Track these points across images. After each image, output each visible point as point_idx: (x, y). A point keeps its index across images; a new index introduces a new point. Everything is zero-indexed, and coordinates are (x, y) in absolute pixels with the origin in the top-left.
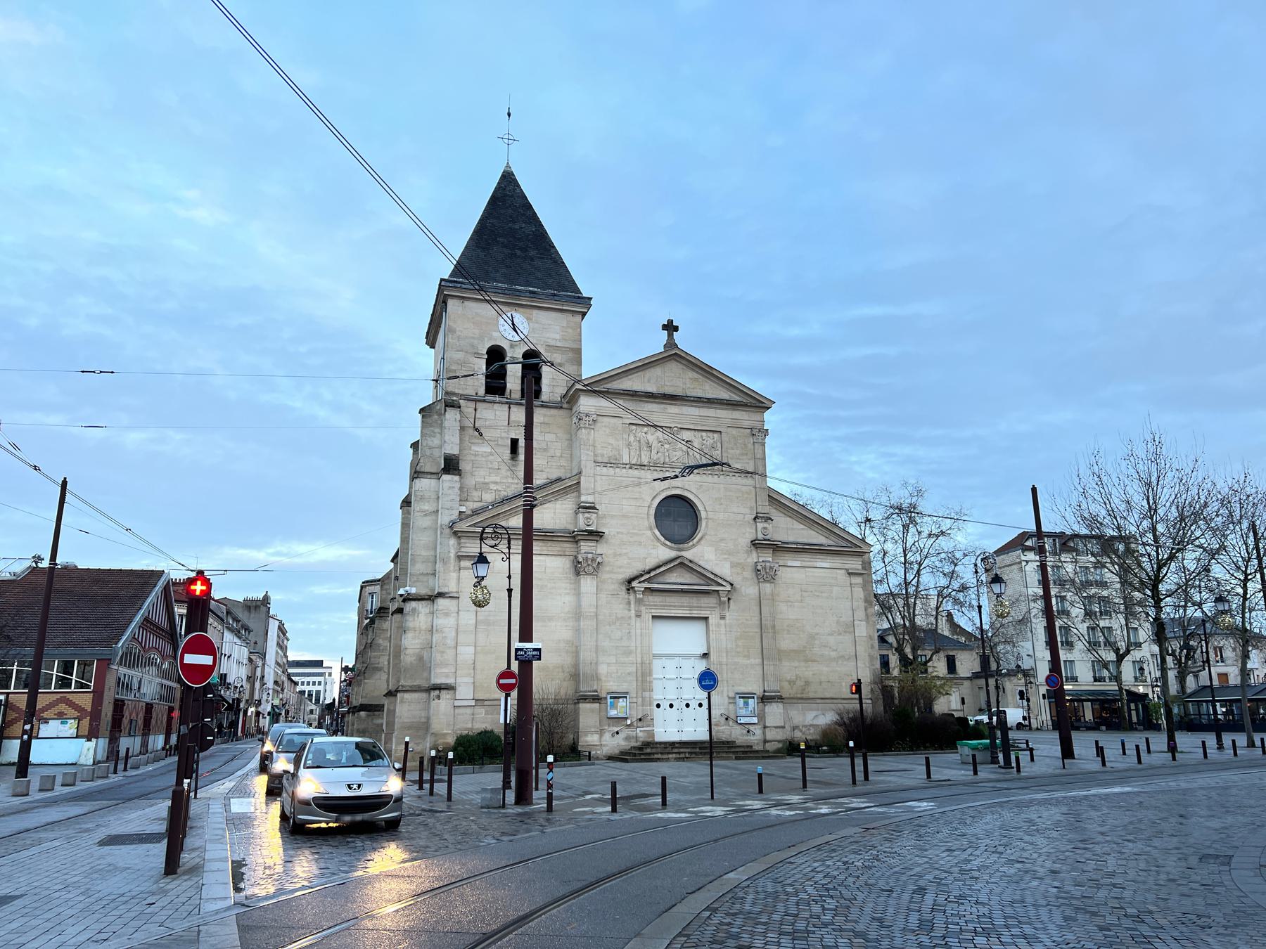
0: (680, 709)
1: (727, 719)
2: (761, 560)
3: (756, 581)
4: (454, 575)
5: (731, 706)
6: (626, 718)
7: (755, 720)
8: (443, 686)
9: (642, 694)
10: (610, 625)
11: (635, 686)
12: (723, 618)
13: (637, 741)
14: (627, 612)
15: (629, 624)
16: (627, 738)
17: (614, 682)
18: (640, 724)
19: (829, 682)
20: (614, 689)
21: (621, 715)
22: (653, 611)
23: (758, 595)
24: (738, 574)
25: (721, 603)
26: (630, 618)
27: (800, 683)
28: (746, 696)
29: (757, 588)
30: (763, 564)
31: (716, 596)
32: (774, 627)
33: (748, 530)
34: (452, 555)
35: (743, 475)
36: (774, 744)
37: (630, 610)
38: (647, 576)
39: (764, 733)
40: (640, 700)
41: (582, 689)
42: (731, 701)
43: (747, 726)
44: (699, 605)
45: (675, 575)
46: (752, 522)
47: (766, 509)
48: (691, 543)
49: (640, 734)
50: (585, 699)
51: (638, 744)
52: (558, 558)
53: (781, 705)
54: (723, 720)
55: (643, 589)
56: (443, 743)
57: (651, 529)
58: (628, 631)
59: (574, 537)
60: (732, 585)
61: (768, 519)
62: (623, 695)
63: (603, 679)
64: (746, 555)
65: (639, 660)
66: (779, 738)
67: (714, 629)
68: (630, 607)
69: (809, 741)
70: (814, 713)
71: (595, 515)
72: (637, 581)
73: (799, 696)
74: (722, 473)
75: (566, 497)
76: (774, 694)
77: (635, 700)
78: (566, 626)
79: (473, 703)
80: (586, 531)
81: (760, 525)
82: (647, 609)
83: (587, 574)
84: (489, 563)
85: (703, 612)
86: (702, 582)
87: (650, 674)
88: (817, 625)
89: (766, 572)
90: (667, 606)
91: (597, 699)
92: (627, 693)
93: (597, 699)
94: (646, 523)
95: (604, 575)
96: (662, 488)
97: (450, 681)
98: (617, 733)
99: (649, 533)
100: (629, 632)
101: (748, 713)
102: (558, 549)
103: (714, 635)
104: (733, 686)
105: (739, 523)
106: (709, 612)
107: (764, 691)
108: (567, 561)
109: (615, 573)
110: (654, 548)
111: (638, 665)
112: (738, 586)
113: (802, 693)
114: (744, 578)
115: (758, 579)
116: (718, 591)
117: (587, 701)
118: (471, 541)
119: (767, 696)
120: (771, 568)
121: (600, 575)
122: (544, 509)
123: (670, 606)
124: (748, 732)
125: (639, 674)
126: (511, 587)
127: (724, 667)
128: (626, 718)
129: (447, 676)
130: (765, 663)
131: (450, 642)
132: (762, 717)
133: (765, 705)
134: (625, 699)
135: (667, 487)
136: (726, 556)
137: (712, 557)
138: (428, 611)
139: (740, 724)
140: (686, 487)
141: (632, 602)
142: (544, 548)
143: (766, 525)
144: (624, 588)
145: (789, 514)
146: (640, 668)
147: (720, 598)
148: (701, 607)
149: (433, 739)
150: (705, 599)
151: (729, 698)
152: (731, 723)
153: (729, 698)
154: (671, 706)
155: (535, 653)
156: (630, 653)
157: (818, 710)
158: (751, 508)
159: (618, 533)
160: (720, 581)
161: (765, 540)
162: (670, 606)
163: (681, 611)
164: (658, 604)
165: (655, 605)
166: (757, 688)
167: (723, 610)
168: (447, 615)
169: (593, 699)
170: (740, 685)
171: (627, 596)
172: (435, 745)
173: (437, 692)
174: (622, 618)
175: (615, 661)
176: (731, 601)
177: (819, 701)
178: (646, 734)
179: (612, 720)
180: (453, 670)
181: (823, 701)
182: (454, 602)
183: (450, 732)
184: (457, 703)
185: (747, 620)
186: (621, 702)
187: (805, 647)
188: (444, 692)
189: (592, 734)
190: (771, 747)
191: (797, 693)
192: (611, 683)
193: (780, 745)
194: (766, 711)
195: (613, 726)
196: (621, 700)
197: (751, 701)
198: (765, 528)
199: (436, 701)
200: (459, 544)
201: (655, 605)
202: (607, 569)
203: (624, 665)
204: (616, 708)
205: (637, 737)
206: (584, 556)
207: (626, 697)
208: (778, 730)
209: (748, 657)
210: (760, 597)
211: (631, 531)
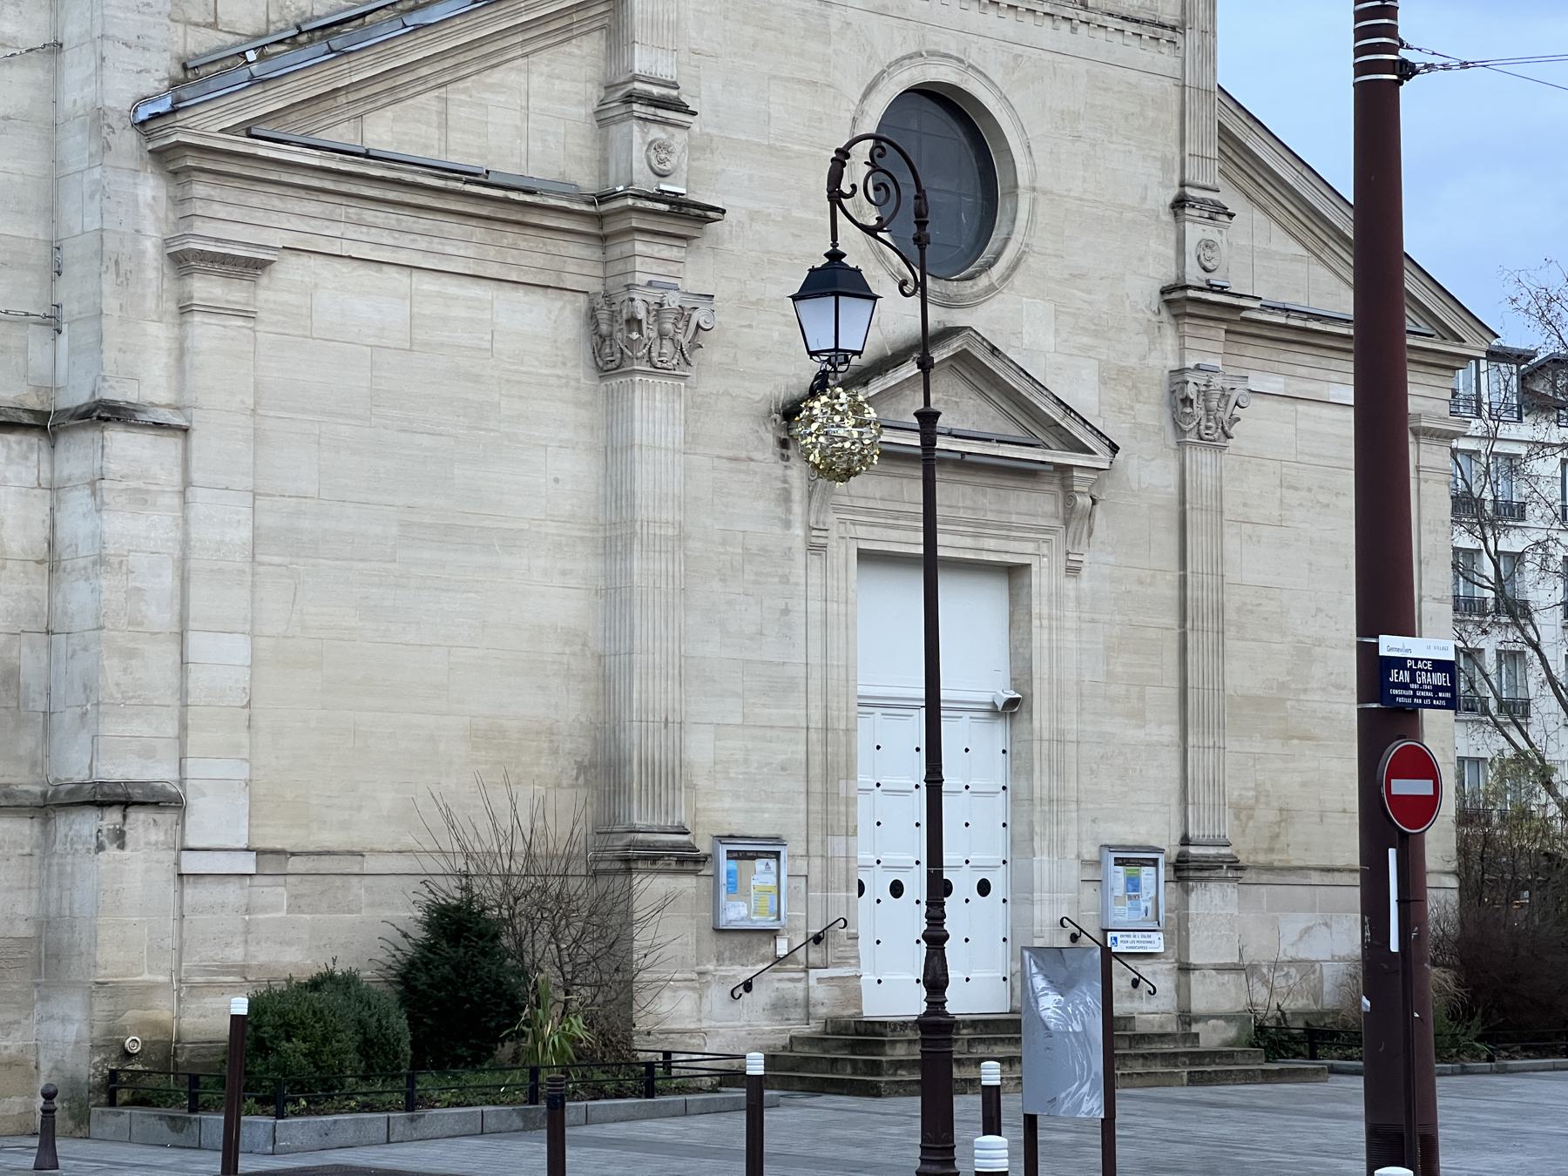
2: (1190, 364)
3: (1172, 442)
4: (159, 333)
5: (1089, 891)
6: (773, 934)
7: (1156, 943)
8: (137, 794)
10: (723, 580)
12: (1073, 571)
13: (808, 1017)
14: (778, 530)
15: (785, 580)
16: (779, 1007)
17: (737, 796)
18: (815, 955)
19: (1344, 811)
20: (737, 823)
22: (861, 531)
23: (1174, 489)
25: (1069, 513)
26: (788, 553)
27: (1265, 815)
28: (1132, 858)
29: (1174, 466)
30: (1201, 378)
31: (1055, 487)
32: (1220, 610)
34: (151, 248)
35: (1147, 32)
36: (1214, 1029)
37: (787, 524)
39: (1182, 990)
41: (638, 822)
42: (1090, 874)
44: (1003, 518)
46: (1167, 217)
47: (1207, 174)
48: (983, 281)
49: (819, 993)
50: (655, 859)
51: (813, 1028)
52: (537, 296)
53: (1231, 890)
56: (141, 1026)
58: (781, 604)
59: (600, 218)
60: (1114, 449)
61: (1218, 212)
62: (768, 849)
63: (702, 782)
66: (1226, 1006)
67: (1045, 611)
68: (789, 511)
69: (1288, 1016)
70: (1301, 921)
71: (680, 136)
73: (1262, 859)
74: (1084, 15)
75: (566, 48)
76: (1212, 851)
78: (564, 573)
79: (247, 864)
80: (660, 197)
81: (1196, 232)
83: (656, 369)
84: (875, 298)
86: (1014, 432)
87: (850, 772)
88: (1319, 610)
89: (1208, 410)
91: (689, 860)
92: (777, 840)
93: (689, 860)
95: (707, 378)
96: (899, 54)
97: (160, 772)
98: (748, 986)
100: (786, 611)
102: (539, 261)
103: (1045, 637)
104: (1094, 821)
105: (1129, 215)
106: (1030, 547)
107: (1185, 841)
108: (567, 312)
113: (1271, 850)
115: (1180, 431)
116: (1065, 470)
117: (660, 865)
118: (231, 195)
119: (1197, 858)
120: (1224, 395)
122: (490, 88)
124: (1135, 983)
125: (816, 771)
126: (934, 406)
127: (1071, 750)
128: (773, 934)
129: (148, 753)
130: (1191, 740)
131: (161, 616)
132: (1179, 932)
133: (1187, 892)
134: (773, 863)
135: (914, 49)
136: (1086, 340)
137: (1049, 341)
138: (31, 479)
140: (974, 58)
142: (491, 253)
143: (1209, 232)
144: (770, 439)
145: (1262, 198)
146: (817, 748)
148: (1009, 527)
149: (102, 1007)
151: (1085, 863)
153: (1085, 863)
155: (1439, 679)
157: (1312, 909)
158: (1165, 162)
159: (753, 216)
160: (1078, 431)
161: (1211, 288)
164: (880, 505)
165: (869, 511)
166: (1160, 832)
168: (141, 498)
169: (681, 861)
171: (778, 469)
172: (110, 1031)
173: (113, 817)
175: (740, 721)
176: (1098, 507)
177: (1316, 878)
179: (727, 937)
180: (171, 729)
181: (1328, 878)
182: (170, 446)
183: (161, 978)
184: (191, 863)
186: (761, 874)
187: (1282, 686)
188: (138, 817)
189: (675, 990)
190: (1211, 1036)
191: (1255, 851)
192: (727, 803)
193: (1231, 1032)
194: (1192, 911)
196: (760, 864)
197: (1146, 873)
198: (1208, 245)
199: (112, 851)
200: (179, 202)
201: (869, 511)
203: (769, 733)
204: (746, 895)
206: (653, 296)
207: (777, 855)
208: (1227, 978)
210: (1183, 502)
211: (796, 213)
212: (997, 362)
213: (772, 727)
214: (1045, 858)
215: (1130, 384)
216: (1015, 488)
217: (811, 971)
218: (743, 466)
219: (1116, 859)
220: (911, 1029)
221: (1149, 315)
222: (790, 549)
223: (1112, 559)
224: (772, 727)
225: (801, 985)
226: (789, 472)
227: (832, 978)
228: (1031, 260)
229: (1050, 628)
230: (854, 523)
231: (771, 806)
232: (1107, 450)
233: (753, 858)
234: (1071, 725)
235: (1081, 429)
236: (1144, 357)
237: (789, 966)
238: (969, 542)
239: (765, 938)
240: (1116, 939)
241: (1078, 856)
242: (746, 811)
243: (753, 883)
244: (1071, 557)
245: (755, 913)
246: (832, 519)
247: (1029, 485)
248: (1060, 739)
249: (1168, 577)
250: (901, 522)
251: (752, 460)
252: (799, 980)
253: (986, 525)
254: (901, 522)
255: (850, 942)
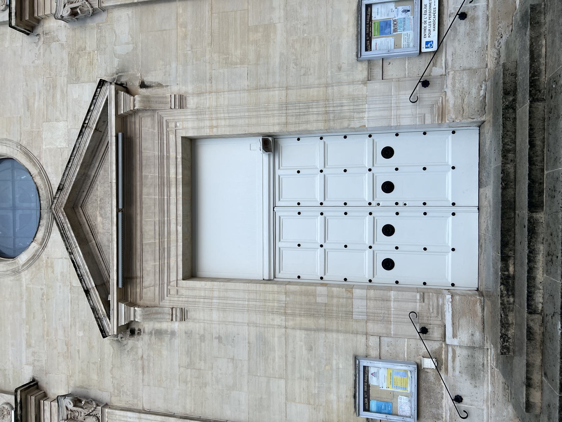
0: (397, 209)
1: (426, 84)
5: (392, 70)
9: (357, 321)
10: (205, 385)
11: (341, 337)
13: (481, 348)
14: (177, 341)
15: (202, 338)
17: (329, 389)
18: (435, 333)
21: (412, 388)
22: (173, 278)
24: (91, 63)
29: (116, 13)
33: (7, 44)
37: (173, 333)
38: (95, 294)
40: (372, 327)
42: (377, 71)
43: (447, 22)
45: (99, 219)
49: (464, 337)
54: (426, 94)
55: (122, 306)
57: (16, 272)
58: (216, 342)
60: (102, 83)
64: (54, 45)
65: (278, 320)
68: (166, 332)
72: (105, 322)
77: (373, 341)
82: (169, 291)
85: (172, 154)
90: (161, 243)
94: (9, 280)
98: (458, 399)
99: (25, 276)
100: (219, 338)
101: (411, 20)
103: (222, 123)
104: (340, 69)
106: (172, 137)
109: (102, 359)
110: (52, 267)
111: (291, 323)
112: (116, 62)
114: (98, 48)
121: (105, 397)
123: (161, 235)
125: (310, 322)
127: (293, 95)
128: (419, 369)
136: (58, 96)
139: (440, 43)
141: (158, 326)
147: (138, 110)
148: (161, 157)
150: (144, 145)
151: (370, 78)
152: (437, 71)
153: (370, 78)
154: (388, 230)
156: (263, 340)
159: (29, 346)
162: (161, 235)
163: (173, 208)
165: (161, 272)
167: (162, 100)
170: (339, 46)
174: (188, 353)
175: (282, 382)
176: (148, 79)
178: (463, 321)
179: (422, 408)
185: (185, 37)
195: (439, 406)
196: (373, 381)
197: (378, 15)
201: (161, 272)
202: (95, 377)
203: (290, 359)
204: (394, 395)
205: (472, 348)
209: (269, 28)
211: (24, 316)
212: (66, 186)
213: (286, 356)
214: (366, 115)
215: (77, 56)
216: (141, 152)
217: (448, 341)
218: (146, 363)
219: (366, 50)
220: (507, 330)
221: (41, 43)
222: (186, 333)
223: (174, 65)
224: (286, 356)
225: (458, 351)
226: (146, 330)
227: (453, 324)
228: (24, 143)
229: (217, 119)
230: (169, 282)
231: (334, 362)
232: (104, 88)
233: (368, 386)
234: (277, 95)
235: (95, 112)
236: (62, 45)
237: (443, 357)
238: (173, 190)
239: (423, 376)
240: (427, 43)
241: (364, 83)
242: (338, 382)
243: (385, 388)
244: (173, 107)
245: (405, 389)
246: (167, 303)
247: (138, 141)
248: (285, 106)
249: (180, 11)
250: (166, 246)
251: (142, 357)
252: (454, 352)
253: (161, 177)
254: (166, 246)
255: (426, 300)
